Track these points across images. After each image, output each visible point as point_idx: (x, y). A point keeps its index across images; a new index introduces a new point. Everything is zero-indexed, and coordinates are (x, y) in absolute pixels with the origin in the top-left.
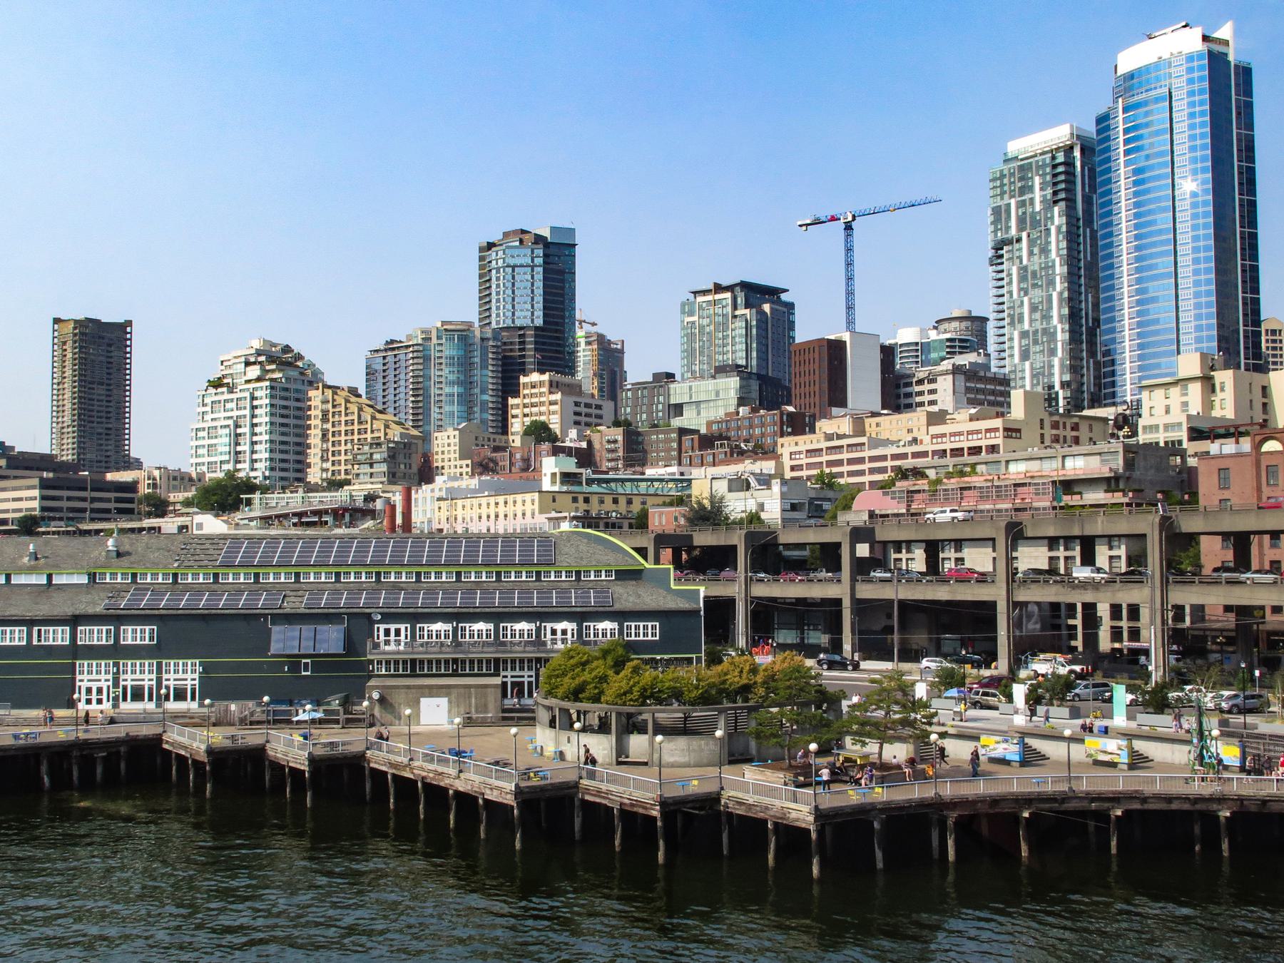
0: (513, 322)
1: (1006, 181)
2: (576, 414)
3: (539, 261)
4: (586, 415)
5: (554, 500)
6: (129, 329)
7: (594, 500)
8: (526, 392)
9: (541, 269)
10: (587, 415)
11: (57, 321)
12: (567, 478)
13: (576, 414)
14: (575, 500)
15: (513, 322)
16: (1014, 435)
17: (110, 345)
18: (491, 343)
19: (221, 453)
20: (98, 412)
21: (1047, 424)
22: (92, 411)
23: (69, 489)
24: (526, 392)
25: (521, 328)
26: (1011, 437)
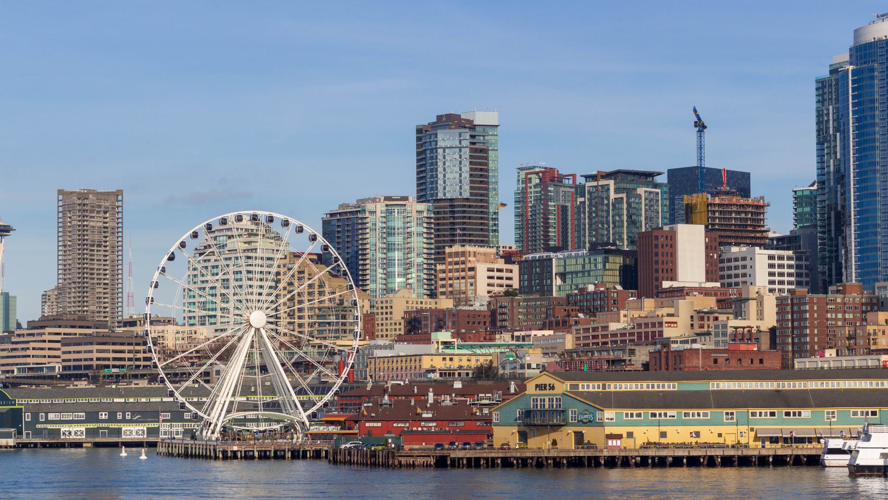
0: (445, 195)
1: (826, 90)
2: (489, 278)
3: (465, 143)
4: (498, 278)
5: (432, 360)
6: (120, 198)
7: (456, 358)
8: (450, 260)
9: (467, 150)
10: (498, 278)
11: (60, 192)
12: (447, 344)
13: (489, 278)
14: (444, 359)
15: (445, 195)
16: (672, 325)
17: (105, 212)
18: (425, 214)
19: (209, 310)
20: (97, 269)
21: (695, 318)
22: (93, 269)
23: (114, 344)
24: (450, 260)
25: (451, 200)
26: (671, 327)
